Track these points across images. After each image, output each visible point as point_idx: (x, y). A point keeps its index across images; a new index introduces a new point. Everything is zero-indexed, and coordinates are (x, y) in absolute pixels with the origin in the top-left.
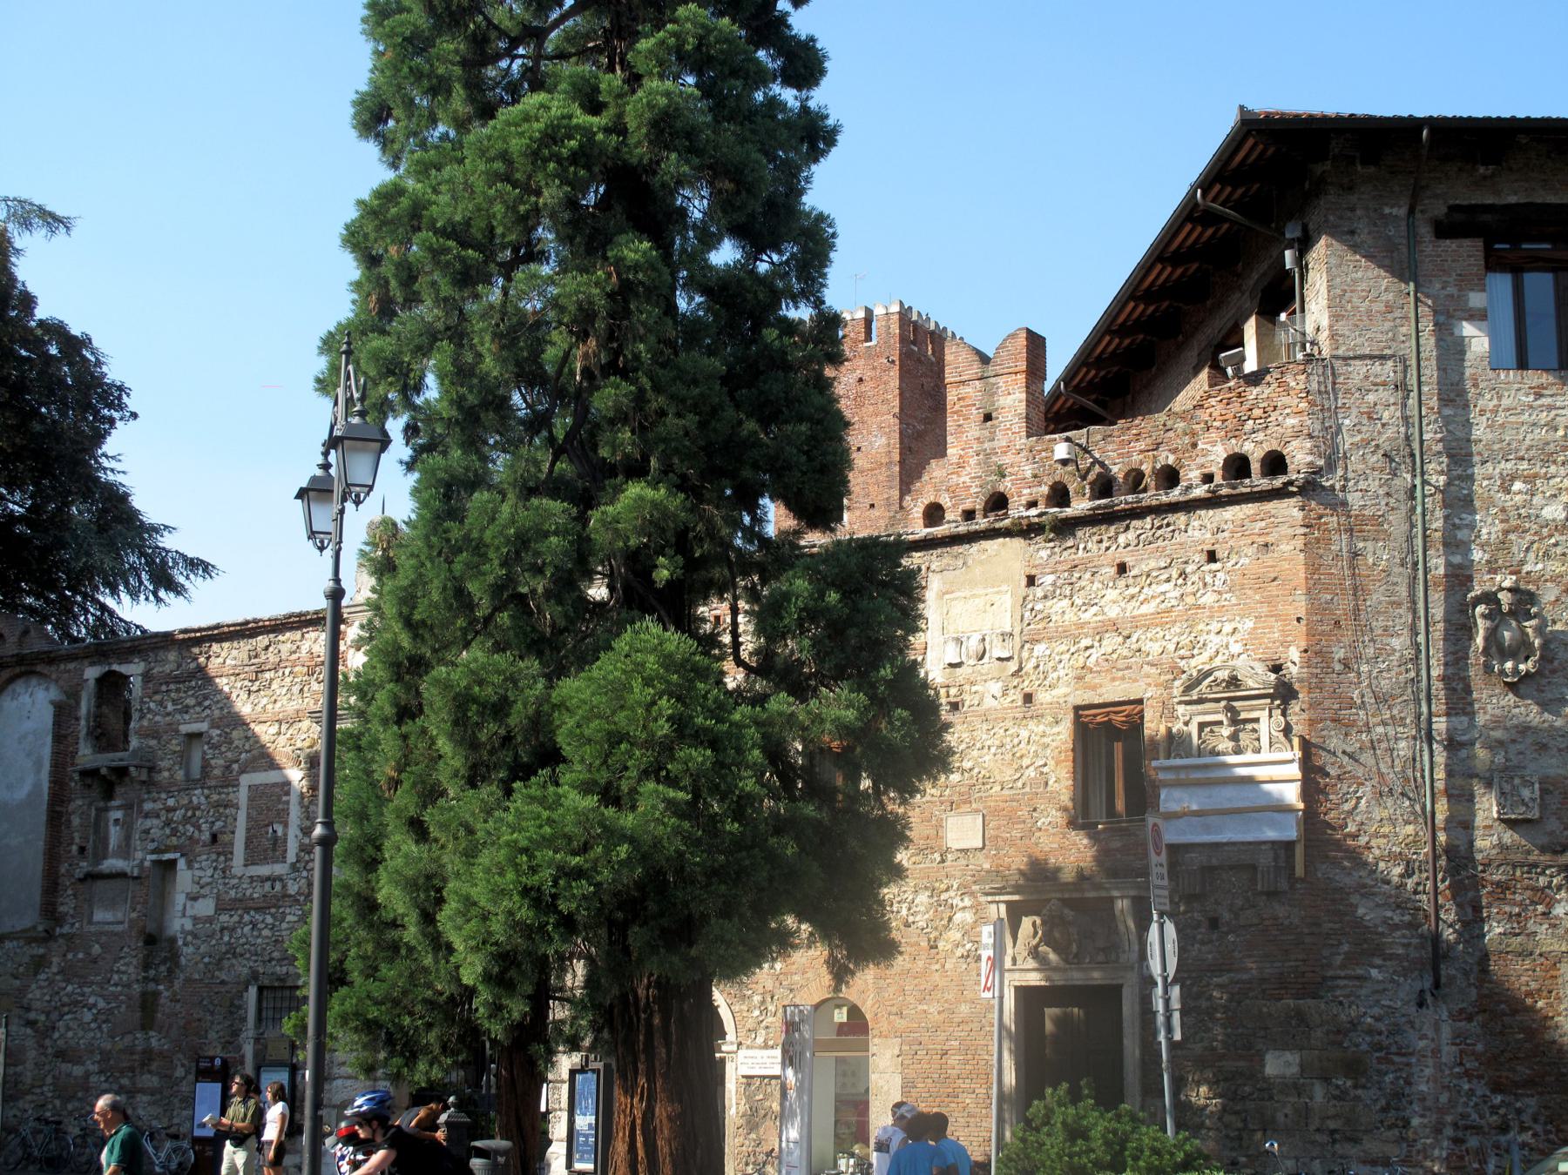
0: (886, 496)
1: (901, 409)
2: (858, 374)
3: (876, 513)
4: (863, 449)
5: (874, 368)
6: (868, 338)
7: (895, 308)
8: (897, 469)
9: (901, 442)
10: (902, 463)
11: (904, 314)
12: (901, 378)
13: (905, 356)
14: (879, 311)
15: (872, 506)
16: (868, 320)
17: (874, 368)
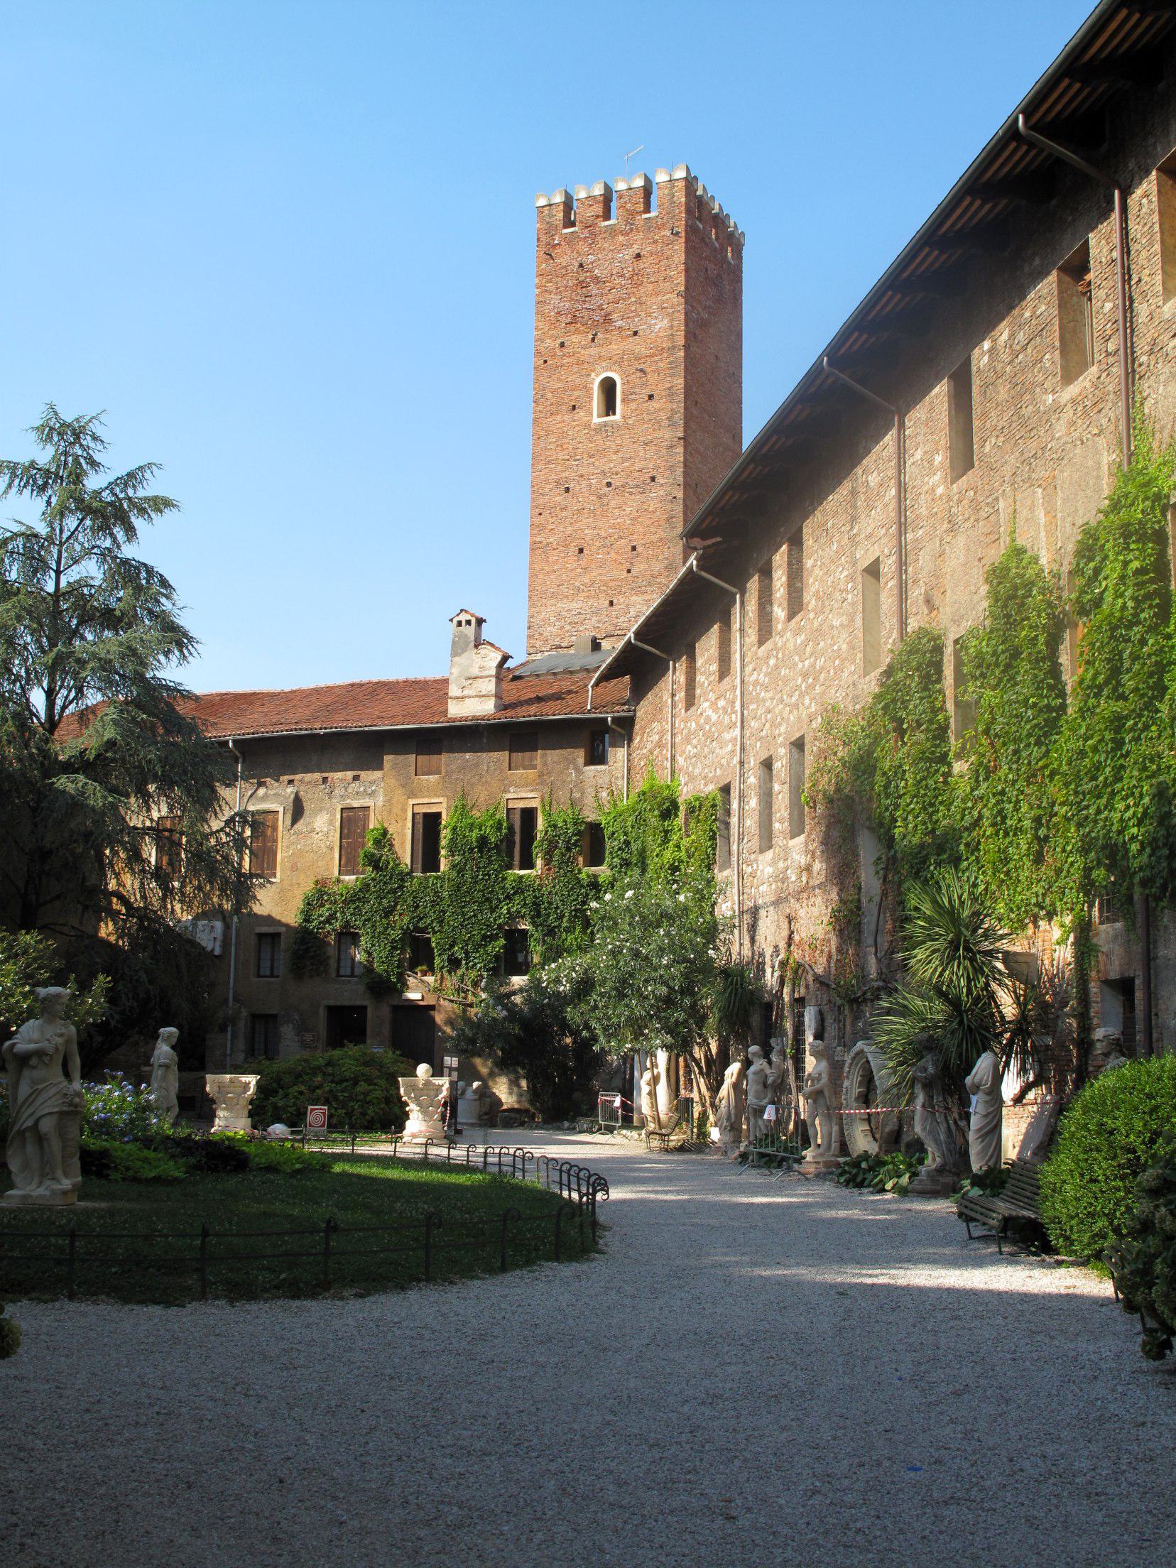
0: (668, 385)
1: (687, 288)
2: (635, 249)
3: (654, 405)
4: (641, 333)
5: (655, 242)
6: (647, 209)
7: (680, 174)
8: (682, 354)
9: (686, 325)
10: (687, 347)
11: (690, 182)
12: (687, 253)
13: (691, 230)
14: (661, 177)
15: (651, 397)
16: (647, 191)
17: (655, 242)
